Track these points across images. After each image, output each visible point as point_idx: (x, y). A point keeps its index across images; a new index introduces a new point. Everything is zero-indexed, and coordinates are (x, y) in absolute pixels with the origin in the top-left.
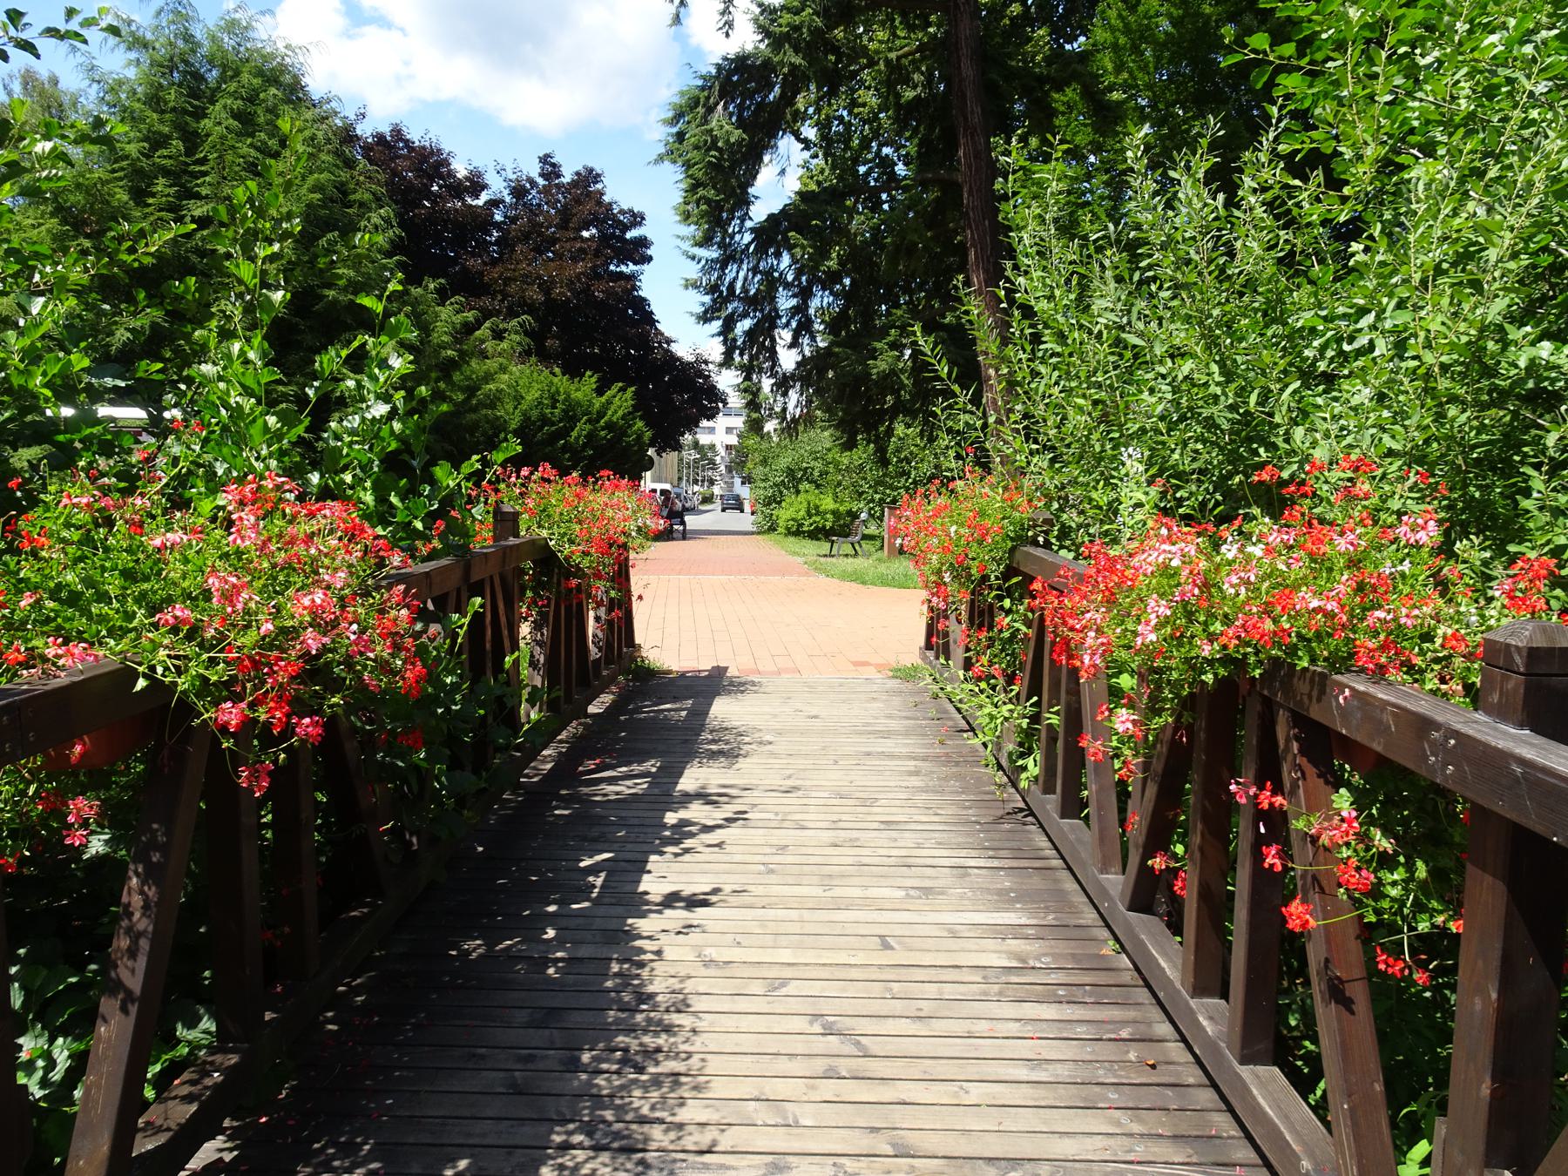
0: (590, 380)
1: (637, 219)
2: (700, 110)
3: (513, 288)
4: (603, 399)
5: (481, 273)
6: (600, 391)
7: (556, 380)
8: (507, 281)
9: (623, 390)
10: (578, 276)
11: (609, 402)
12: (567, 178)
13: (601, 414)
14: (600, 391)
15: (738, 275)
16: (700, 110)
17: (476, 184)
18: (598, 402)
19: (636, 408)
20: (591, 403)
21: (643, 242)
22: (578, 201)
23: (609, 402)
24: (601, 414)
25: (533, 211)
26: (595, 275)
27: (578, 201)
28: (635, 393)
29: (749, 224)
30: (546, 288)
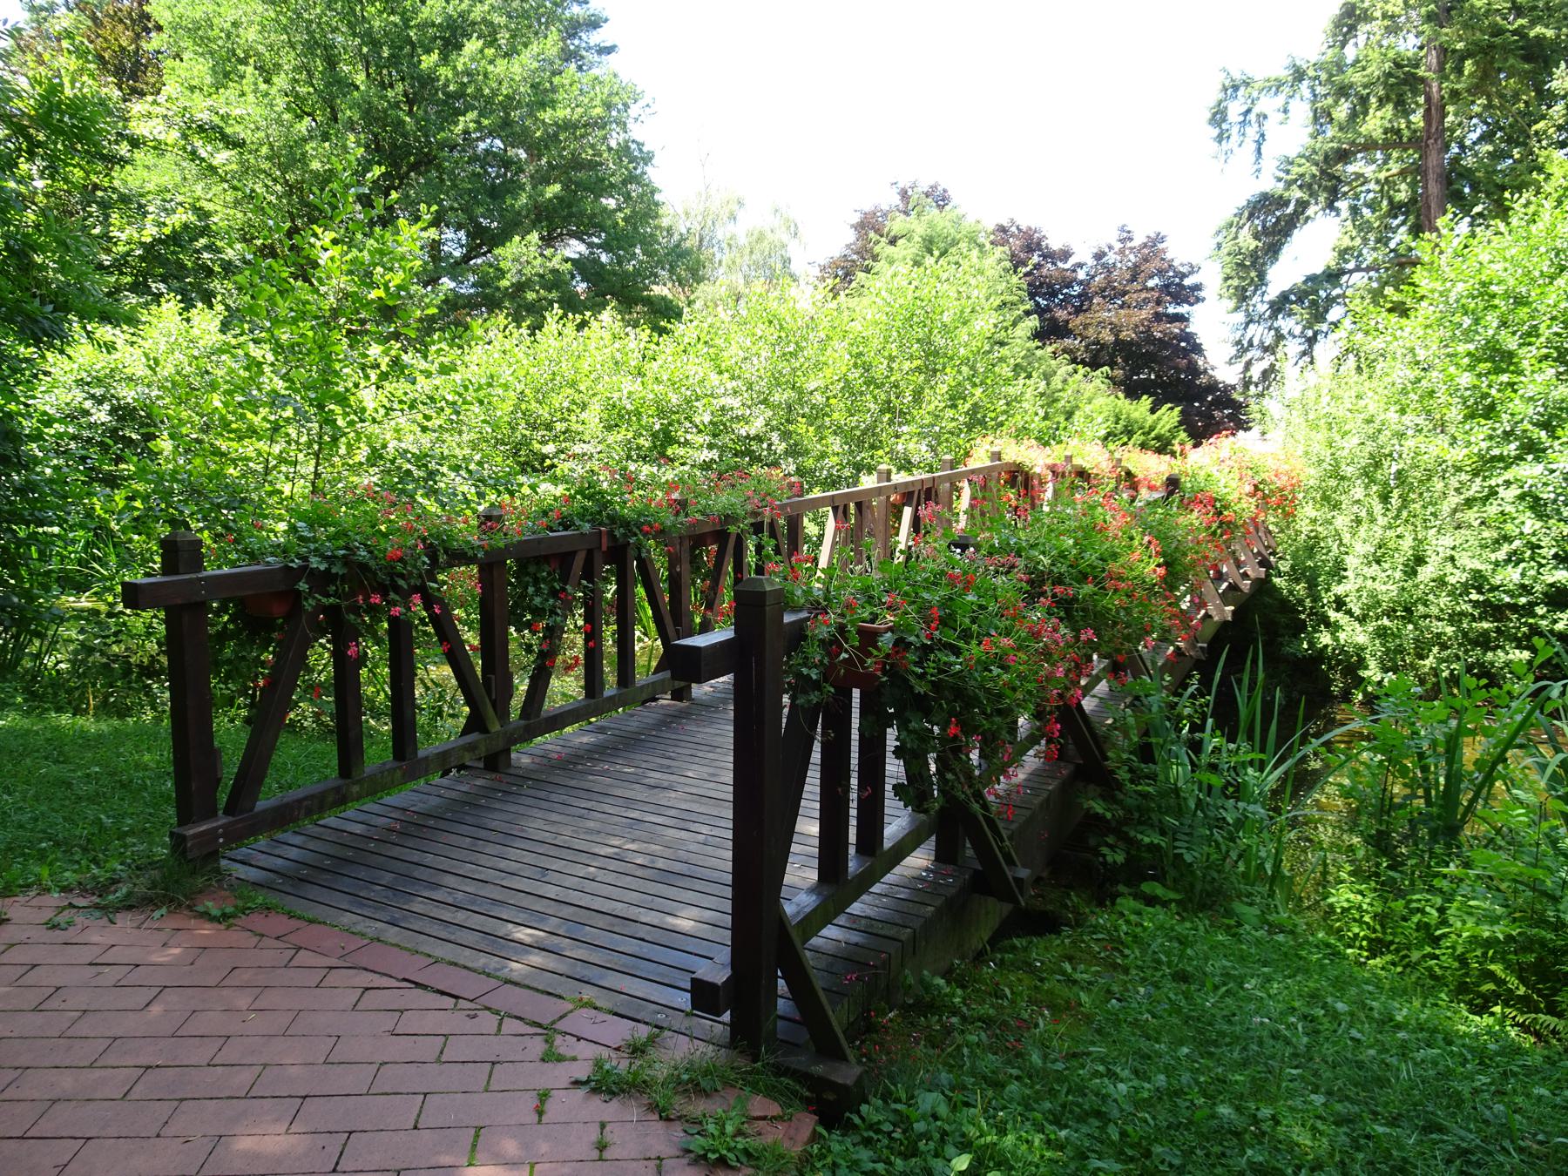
0: (1146, 401)
1: (1193, 270)
2: (1234, 230)
3: (1091, 332)
4: (1155, 417)
5: (1067, 322)
6: (1153, 411)
7: (1120, 403)
8: (1086, 327)
9: (1172, 409)
10: (1142, 321)
11: (1159, 419)
12: (1136, 243)
13: (1152, 429)
14: (1153, 411)
15: (1257, 332)
16: (1234, 230)
17: (1065, 255)
18: (1151, 419)
19: (1181, 423)
20: (1145, 420)
21: (1198, 287)
22: (1146, 260)
23: (1159, 419)
24: (1152, 429)
25: (1109, 269)
26: (1158, 317)
27: (1146, 260)
28: (1181, 412)
29: (1267, 298)
30: (1116, 330)
